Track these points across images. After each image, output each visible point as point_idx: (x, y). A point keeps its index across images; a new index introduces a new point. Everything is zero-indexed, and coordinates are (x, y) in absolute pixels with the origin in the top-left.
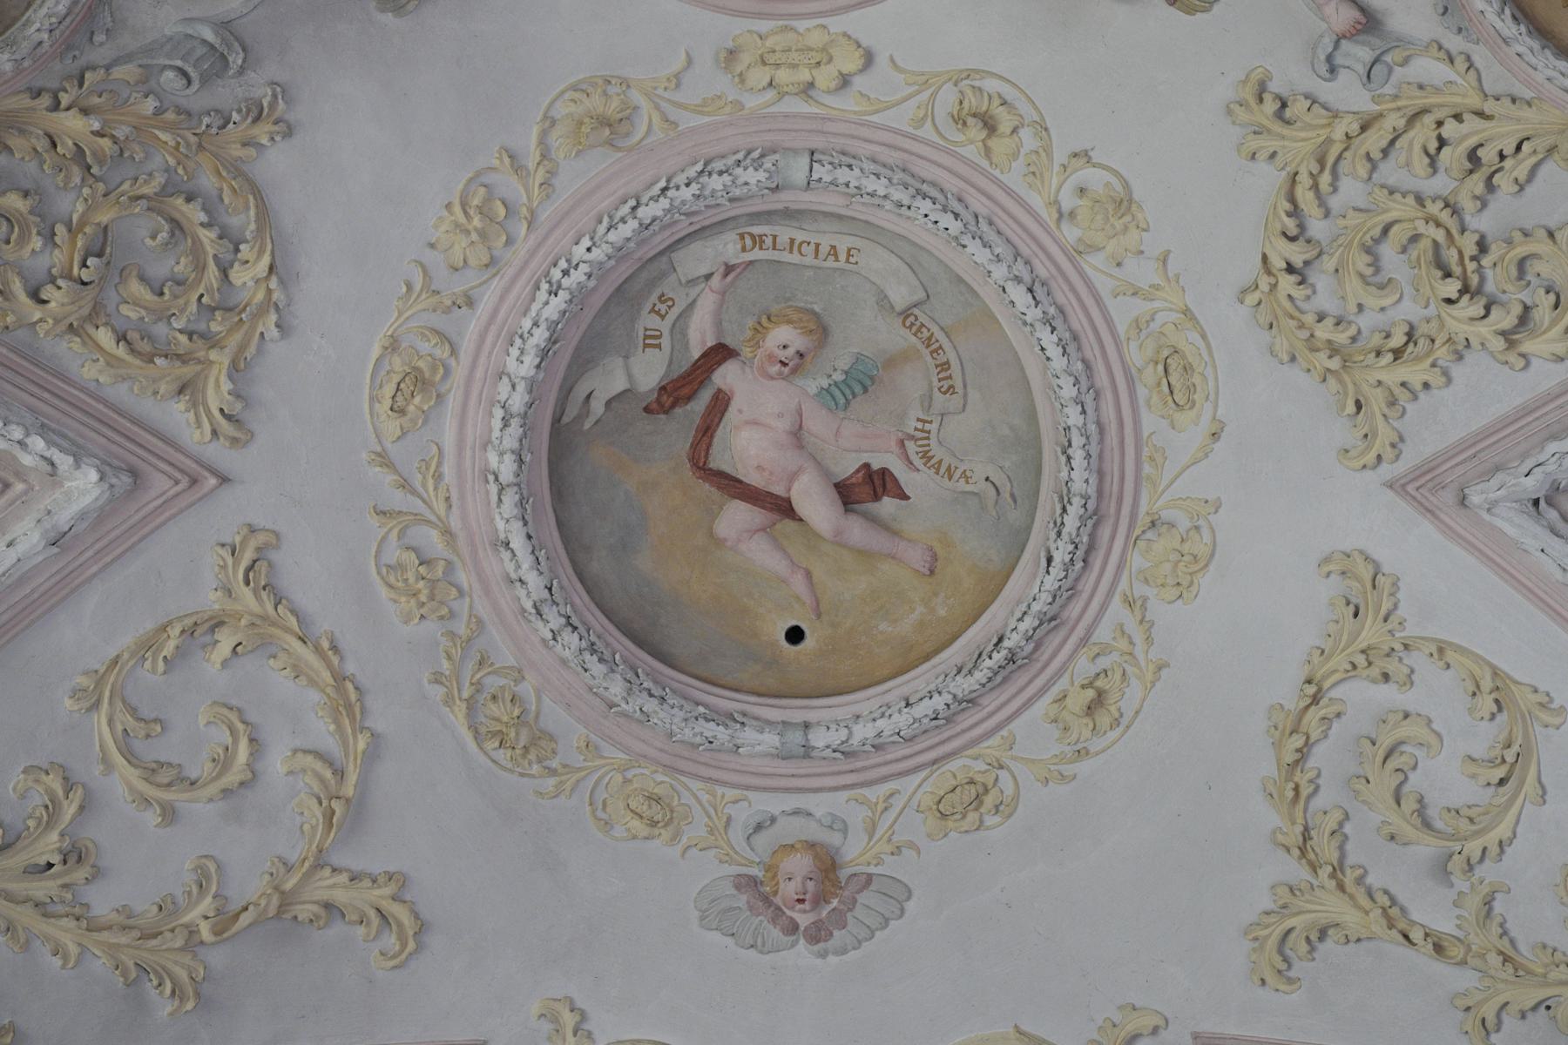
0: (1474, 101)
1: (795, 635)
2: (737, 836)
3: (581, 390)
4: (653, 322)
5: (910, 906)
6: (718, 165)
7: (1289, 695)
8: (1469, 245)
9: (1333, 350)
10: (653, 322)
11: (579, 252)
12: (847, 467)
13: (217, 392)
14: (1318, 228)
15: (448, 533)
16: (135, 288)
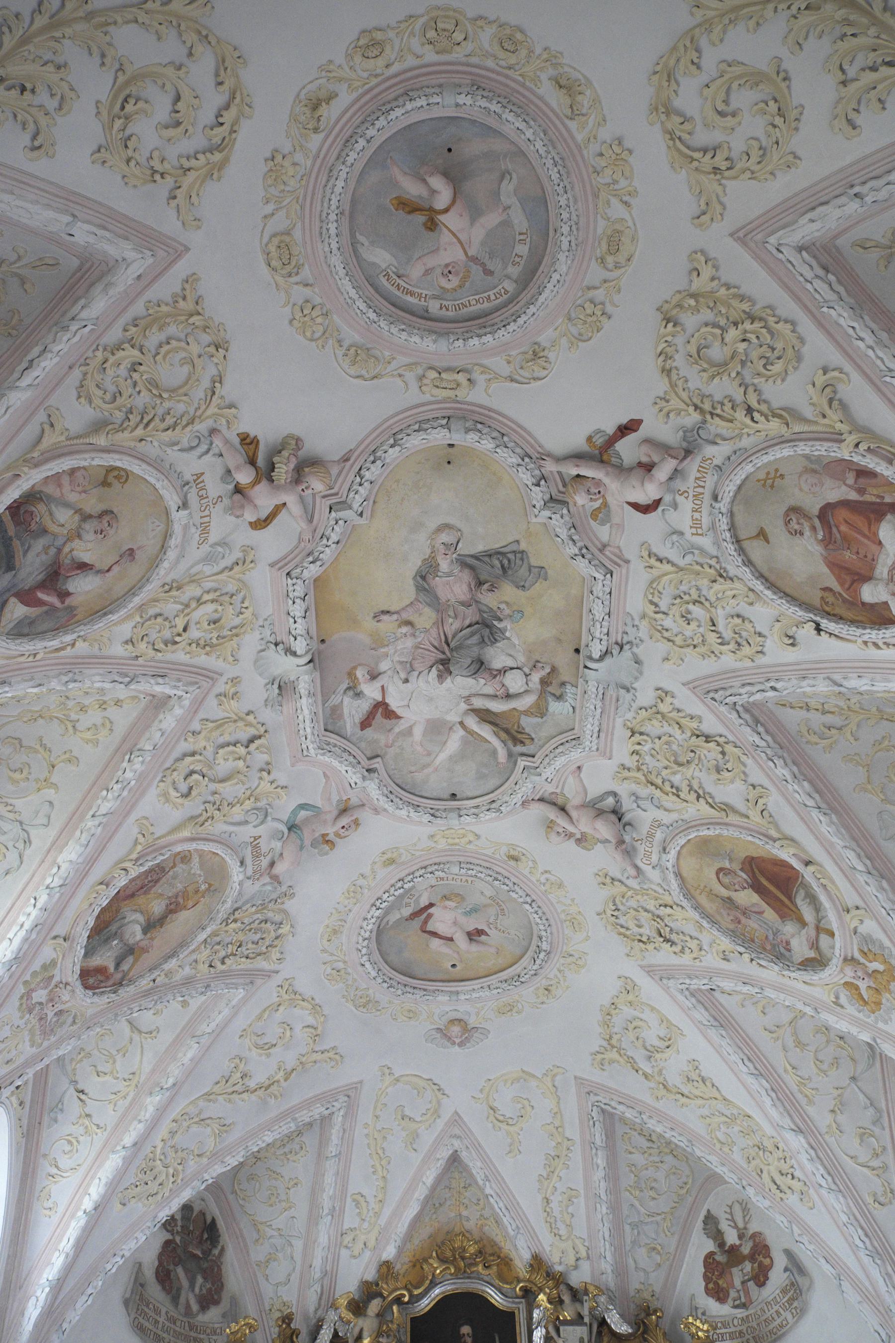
0: (670, 903)
1: (454, 966)
2: (436, 1018)
3: (385, 920)
4: (408, 901)
5: (490, 1036)
6: (430, 870)
7: (606, 1002)
8: (668, 929)
9: (625, 936)
10: (408, 901)
11: (385, 896)
12: (471, 928)
13: (275, 954)
14: (621, 907)
15: (345, 962)
16: (250, 946)
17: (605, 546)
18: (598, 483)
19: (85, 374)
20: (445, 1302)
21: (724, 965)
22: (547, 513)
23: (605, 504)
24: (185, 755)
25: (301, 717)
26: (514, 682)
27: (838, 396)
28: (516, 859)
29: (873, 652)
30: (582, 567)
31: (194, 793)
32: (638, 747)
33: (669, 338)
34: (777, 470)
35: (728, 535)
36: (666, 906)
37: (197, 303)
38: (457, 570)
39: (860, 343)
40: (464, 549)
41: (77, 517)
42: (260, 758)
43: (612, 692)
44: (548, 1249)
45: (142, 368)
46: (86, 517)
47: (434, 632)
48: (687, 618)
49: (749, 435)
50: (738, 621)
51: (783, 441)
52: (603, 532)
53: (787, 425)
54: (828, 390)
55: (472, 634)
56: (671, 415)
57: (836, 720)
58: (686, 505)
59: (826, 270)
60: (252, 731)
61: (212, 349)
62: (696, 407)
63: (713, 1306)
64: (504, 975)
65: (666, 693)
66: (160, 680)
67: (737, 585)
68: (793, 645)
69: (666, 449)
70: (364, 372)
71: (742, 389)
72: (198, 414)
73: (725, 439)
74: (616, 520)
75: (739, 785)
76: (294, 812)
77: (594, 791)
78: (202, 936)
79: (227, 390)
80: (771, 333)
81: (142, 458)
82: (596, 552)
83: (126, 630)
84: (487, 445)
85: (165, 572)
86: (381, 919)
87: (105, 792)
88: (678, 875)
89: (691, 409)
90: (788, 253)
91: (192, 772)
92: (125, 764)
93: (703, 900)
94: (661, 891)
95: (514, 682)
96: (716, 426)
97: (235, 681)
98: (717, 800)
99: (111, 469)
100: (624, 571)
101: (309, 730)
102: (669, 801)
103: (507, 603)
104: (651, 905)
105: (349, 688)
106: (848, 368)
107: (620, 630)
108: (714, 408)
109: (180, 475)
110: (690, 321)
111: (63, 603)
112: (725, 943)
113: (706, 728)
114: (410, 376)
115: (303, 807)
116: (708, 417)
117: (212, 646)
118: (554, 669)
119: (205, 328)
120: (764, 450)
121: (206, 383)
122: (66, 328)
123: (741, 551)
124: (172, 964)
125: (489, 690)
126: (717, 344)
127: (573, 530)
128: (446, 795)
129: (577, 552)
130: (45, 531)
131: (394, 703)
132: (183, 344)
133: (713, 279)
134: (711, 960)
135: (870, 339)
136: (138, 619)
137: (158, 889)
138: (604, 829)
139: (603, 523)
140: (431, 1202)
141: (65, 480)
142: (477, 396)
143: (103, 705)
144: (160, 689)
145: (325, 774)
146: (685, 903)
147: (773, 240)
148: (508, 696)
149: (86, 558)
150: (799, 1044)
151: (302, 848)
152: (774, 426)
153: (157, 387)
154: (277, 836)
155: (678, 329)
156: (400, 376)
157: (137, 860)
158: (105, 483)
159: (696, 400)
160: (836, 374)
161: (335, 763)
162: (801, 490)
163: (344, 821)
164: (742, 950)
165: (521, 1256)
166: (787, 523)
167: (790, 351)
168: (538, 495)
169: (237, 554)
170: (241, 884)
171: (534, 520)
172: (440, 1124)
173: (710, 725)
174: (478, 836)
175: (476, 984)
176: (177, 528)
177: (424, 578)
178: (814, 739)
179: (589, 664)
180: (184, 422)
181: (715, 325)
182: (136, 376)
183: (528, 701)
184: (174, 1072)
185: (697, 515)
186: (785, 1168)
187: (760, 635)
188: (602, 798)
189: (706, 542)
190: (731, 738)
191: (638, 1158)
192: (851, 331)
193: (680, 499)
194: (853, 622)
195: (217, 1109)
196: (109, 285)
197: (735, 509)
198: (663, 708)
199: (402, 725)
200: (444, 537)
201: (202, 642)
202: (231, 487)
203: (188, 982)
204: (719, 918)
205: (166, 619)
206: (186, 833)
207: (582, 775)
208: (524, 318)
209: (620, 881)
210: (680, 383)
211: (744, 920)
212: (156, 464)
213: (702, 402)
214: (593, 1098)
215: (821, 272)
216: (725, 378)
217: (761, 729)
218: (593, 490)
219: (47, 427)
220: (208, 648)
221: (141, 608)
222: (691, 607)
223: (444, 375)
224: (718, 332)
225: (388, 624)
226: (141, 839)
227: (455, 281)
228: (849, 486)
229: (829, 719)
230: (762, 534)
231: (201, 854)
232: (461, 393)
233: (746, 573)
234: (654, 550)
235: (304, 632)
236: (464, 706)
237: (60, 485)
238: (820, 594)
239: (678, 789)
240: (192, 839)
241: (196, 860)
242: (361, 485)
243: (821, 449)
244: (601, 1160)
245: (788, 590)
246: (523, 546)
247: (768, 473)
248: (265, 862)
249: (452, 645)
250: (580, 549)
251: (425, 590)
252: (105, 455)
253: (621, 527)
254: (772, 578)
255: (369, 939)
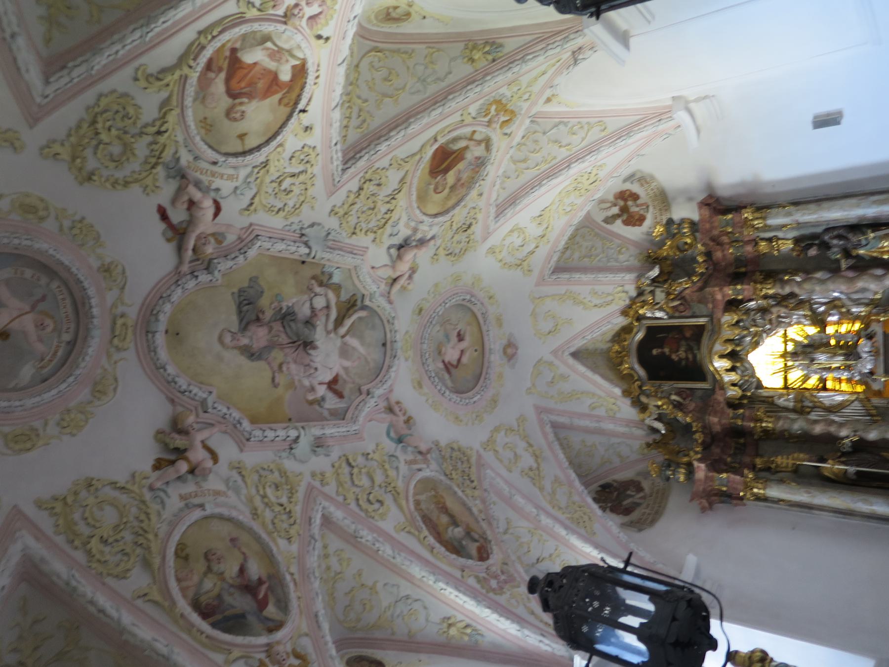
1: (476, 350)
8: (464, 226)
17: (239, 238)
18: (199, 238)
19: (109, 575)
20: (642, 362)
21: (485, 196)
22: (216, 273)
23: (213, 235)
24: (359, 505)
25: (336, 434)
26: (319, 302)
27: (155, 74)
28: (421, 310)
29: (321, 81)
30: (252, 253)
31: (380, 499)
32: (363, 231)
33: (103, 179)
34: (201, 121)
35: (240, 159)
36: (452, 226)
37: (57, 499)
38: (248, 334)
39: (121, 53)
40: (235, 327)
41: (210, 575)
42: (360, 460)
43: (330, 243)
44: (617, 307)
45: (105, 536)
46: (209, 569)
47: (287, 350)
48: (288, 192)
49: (175, 136)
50: (294, 160)
51: (183, 114)
52: (231, 238)
53: (172, 110)
54: (151, 80)
55: (290, 327)
56: (157, 184)
57: (355, 110)
58: (217, 183)
59: (63, 67)
60: (344, 465)
61: (92, 489)
62: (153, 167)
63: (647, 223)
64: (481, 321)
65: (332, 210)
66: (313, 520)
67: (271, 157)
68: (311, 129)
69: (180, 190)
70: (112, 387)
71: (145, 136)
72: (138, 498)
73: (176, 152)
74: (223, 229)
75: (389, 173)
76: (392, 439)
77: (385, 260)
78: (460, 493)
79: (122, 478)
80: (105, 111)
81: (169, 534)
82: (243, 243)
83: (282, 543)
84: (168, 307)
85: (245, 517)
86: (451, 391)
87: (380, 552)
88: (436, 215)
89: (154, 171)
90: (50, 90)
91: (369, 501)
92: (363, 540)
93: (451, 203)
94: (443, 228)
95: (319, 302)
96: (167, 155)
97: (313, 475)
98: (396, 187)
99: (177, 554)
100: (257, 227)
101: (344, 429)
102: (395, 216)
103: (271, 304)
104: (450, 234)
105: (319, 404)
106: (136, 64)
107: (292, 234)
108: (154, 156)
109: (181, 510)
110: (91, 164)
111: (264, 583)
112: (474, 193)
113: (355, 189)
114: (116, 356)
115: (388, 434)
116: (160, 161)
117: (292, 489)
118: (314, 277)
119: (76, 493)
120: (187, 127)
121: (116, 494)
122: (75, 589)
123: (251, 151)
124: (475, 510)
125: (323, 319)
126: (110, 148)
127: (228, 257)
128: (383, 349)
129: (242, 256)
130: (219, 597)
131: (328, 377)
132: (88, 508)
133: (62, 145)
134: (482, 203)
135: (118, 47)
136: (275, 534)
137: (434, 518)
138: (409, 256)
139: (225, 238)
140: (594, 369)
141: (184, 584)
142: (133, 312)
143: (326, 556)
144: (318, 520)
145: (370, 421)
146: (451, 214)
147: (38, 100)
148: (328, 307)
149: (236, 569)
150: (524, 160)
151: (411, 435)
152: (172, 118)
153: (118, 526)
154: (404, 450)
155: (97, 173)
156: (116, 363)
157: (419, 531)
158: (186, 558)
159: (150, 166)
160: (140, 73)
161: (363, 414)
162: (215, 108)
163: (397, 409)
164: (478, 185)
165: (622, 321)
166: (235, 120)
167: (121, 100)
168: (204, 277)
169: (234, 473)
170: (432, 471)
171: (220, 281)
172: (556, 362)
173: (354, 185)
174: (407, 332)
175: (486, 339)
176: (217, 510)
177: (252, 355)
178: (365, 125)
179: (312, 255)
180: (143, 507)
181: (96, 147)
182: (110, 540)
183: (331, 295)
184: (530, 509)
185: (225, 177)
186: (586, 176)
187: (303, 147)
188: (390, 256)
189: (243, 173)
190: (362, 174)
191: (576, 255)
192: (111, 58)
193: (214, 186)
194: (302, 88)
195: (548, 484)
196: (43, 560)
197: (223, 151)
198: (341, 212)
199: (342, 373)
200: (228, 339)
201: (290, 495)
202: (190, 477)
203: (484, 501)
204: (460, 196)
205: (275, 517)
206: (404, 503)
207: (377, 266)
208: (80, 276)
209: (437, 249)
210: (136, 176)
211: (462, 182)
212: (173, 525)
213: (150, 163)
214: (546, 277)
215: (65, 72)
216: (135, 146)
217: (358, 156)
218: (203, 241)
219: (147, 598)
220: (294, 491)
221: (270, 534)
222: (283, 188)
223: (117, 333)
224: (101, 146)
225: (281, 379)
226: (407, 530)
227: (49, 322)
228: (217, 76)
229: (354, 115)
230: (242, 137)
231: (415, 494)
232: (130, 323)
233: (265, 151)
234: (245, 206)
235: (285, 431)
236: (332, 335)
237: (188, 588)
238: (282, 107)
239: (389, 210)
240: (407, 500)
241: (418, 497)
242: (190, 392)
243: (191, 90)
244: (577, 276)
245: (279, 126)
246: (235, 290)
247: (202, 127)
248: (419, 457)
249: (295, 339)
250: (241, 254)
251: (260, 354)
252: (167, 559)
253: (229, 226)
254: (270, 135)
255: (461, 398)
